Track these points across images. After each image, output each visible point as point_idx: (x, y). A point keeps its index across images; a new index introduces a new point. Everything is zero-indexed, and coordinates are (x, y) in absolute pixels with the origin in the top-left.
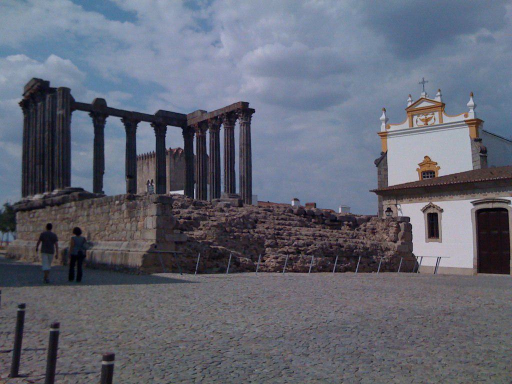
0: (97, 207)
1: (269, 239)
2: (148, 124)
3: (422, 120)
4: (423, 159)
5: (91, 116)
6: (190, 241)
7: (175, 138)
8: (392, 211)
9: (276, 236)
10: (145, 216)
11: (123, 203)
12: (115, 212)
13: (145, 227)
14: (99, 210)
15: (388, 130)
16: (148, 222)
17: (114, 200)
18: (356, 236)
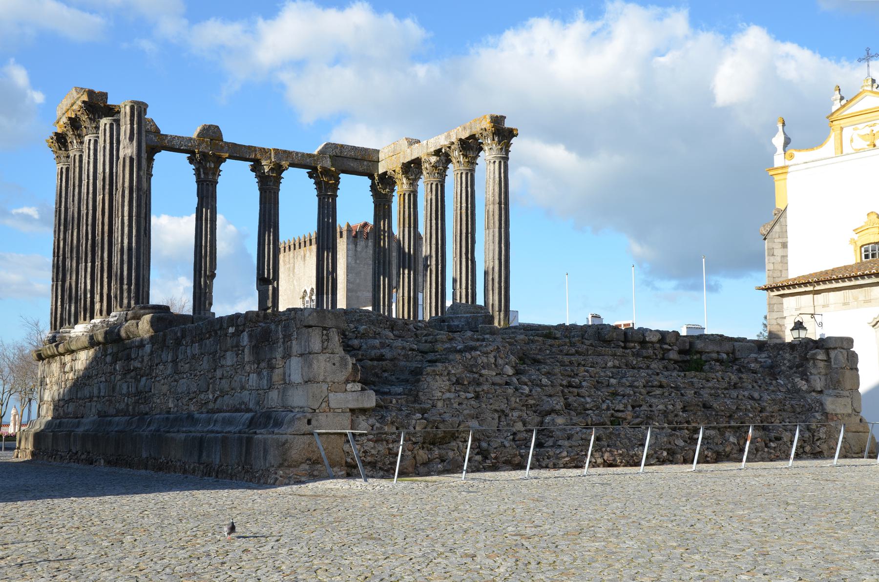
0: (193, 342)
1: (550, 396)
2: (304, 172)
3: (863, 137)
4: (865, 218)
5: (191, 163)
6: (381, 407)
7: (355, 202)
8: (805, 329)
9: (566, 390)
10: (287, 356)
11: (244, 331)
12: (226, 351)
13: (287, 379)
14: (196, 349)
15: (788, 163)
16: (292, 368)
17: (225, 325)
18: (735, 384)
